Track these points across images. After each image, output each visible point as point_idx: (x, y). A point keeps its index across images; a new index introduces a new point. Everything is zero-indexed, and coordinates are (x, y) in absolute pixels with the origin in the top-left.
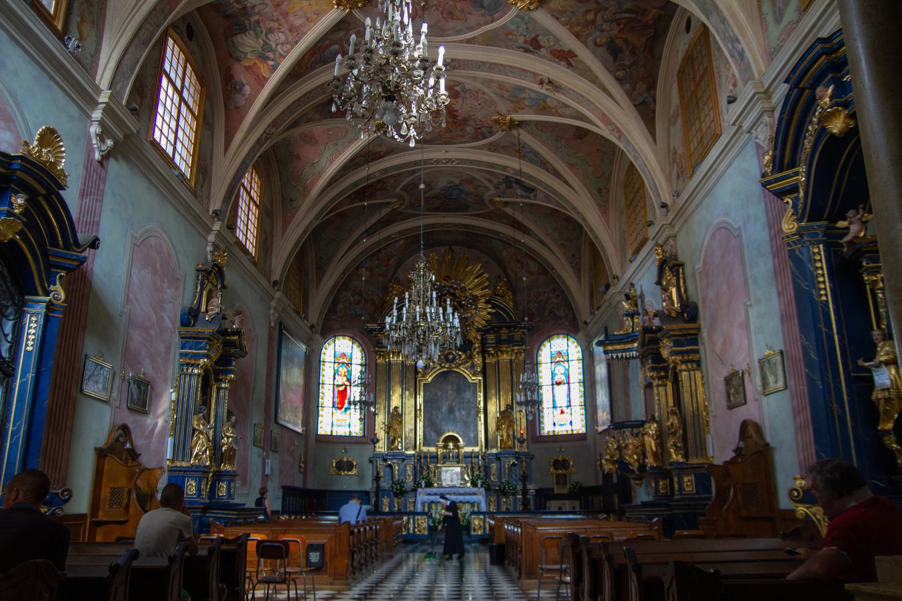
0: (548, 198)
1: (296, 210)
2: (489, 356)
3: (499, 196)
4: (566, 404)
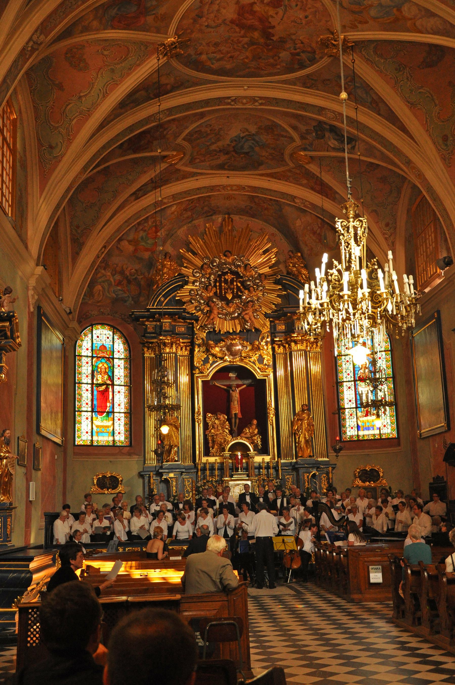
0: (370, 150)
1: (58, 159)
3: (305, 149)
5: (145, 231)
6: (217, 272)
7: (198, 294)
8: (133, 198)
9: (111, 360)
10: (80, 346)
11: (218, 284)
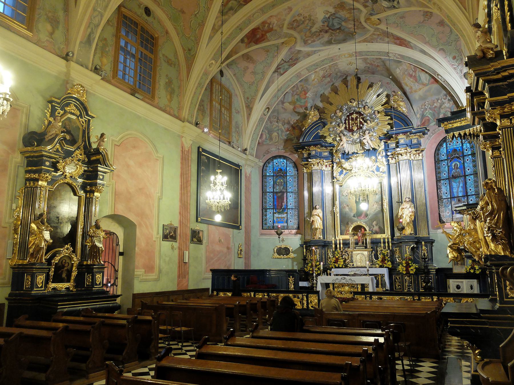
5: (298, 95)
8: (276, 74)
11: (347, 122)
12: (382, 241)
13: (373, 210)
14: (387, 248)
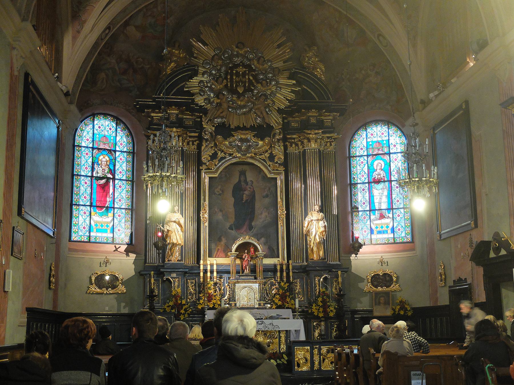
2: (291, 146)
4: (384, 206)
6: (229, 63)
7: (207, 87)
9: (113, 153)
10: (80, 136)
11: (229, 77)
12: (278, 268)
13: (261, 221)
14: (285, 280)
